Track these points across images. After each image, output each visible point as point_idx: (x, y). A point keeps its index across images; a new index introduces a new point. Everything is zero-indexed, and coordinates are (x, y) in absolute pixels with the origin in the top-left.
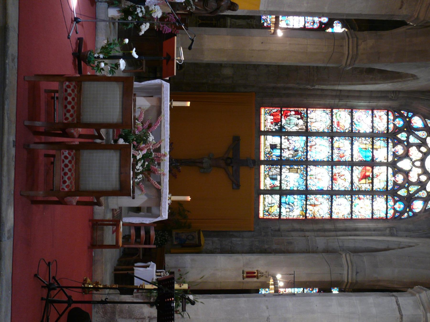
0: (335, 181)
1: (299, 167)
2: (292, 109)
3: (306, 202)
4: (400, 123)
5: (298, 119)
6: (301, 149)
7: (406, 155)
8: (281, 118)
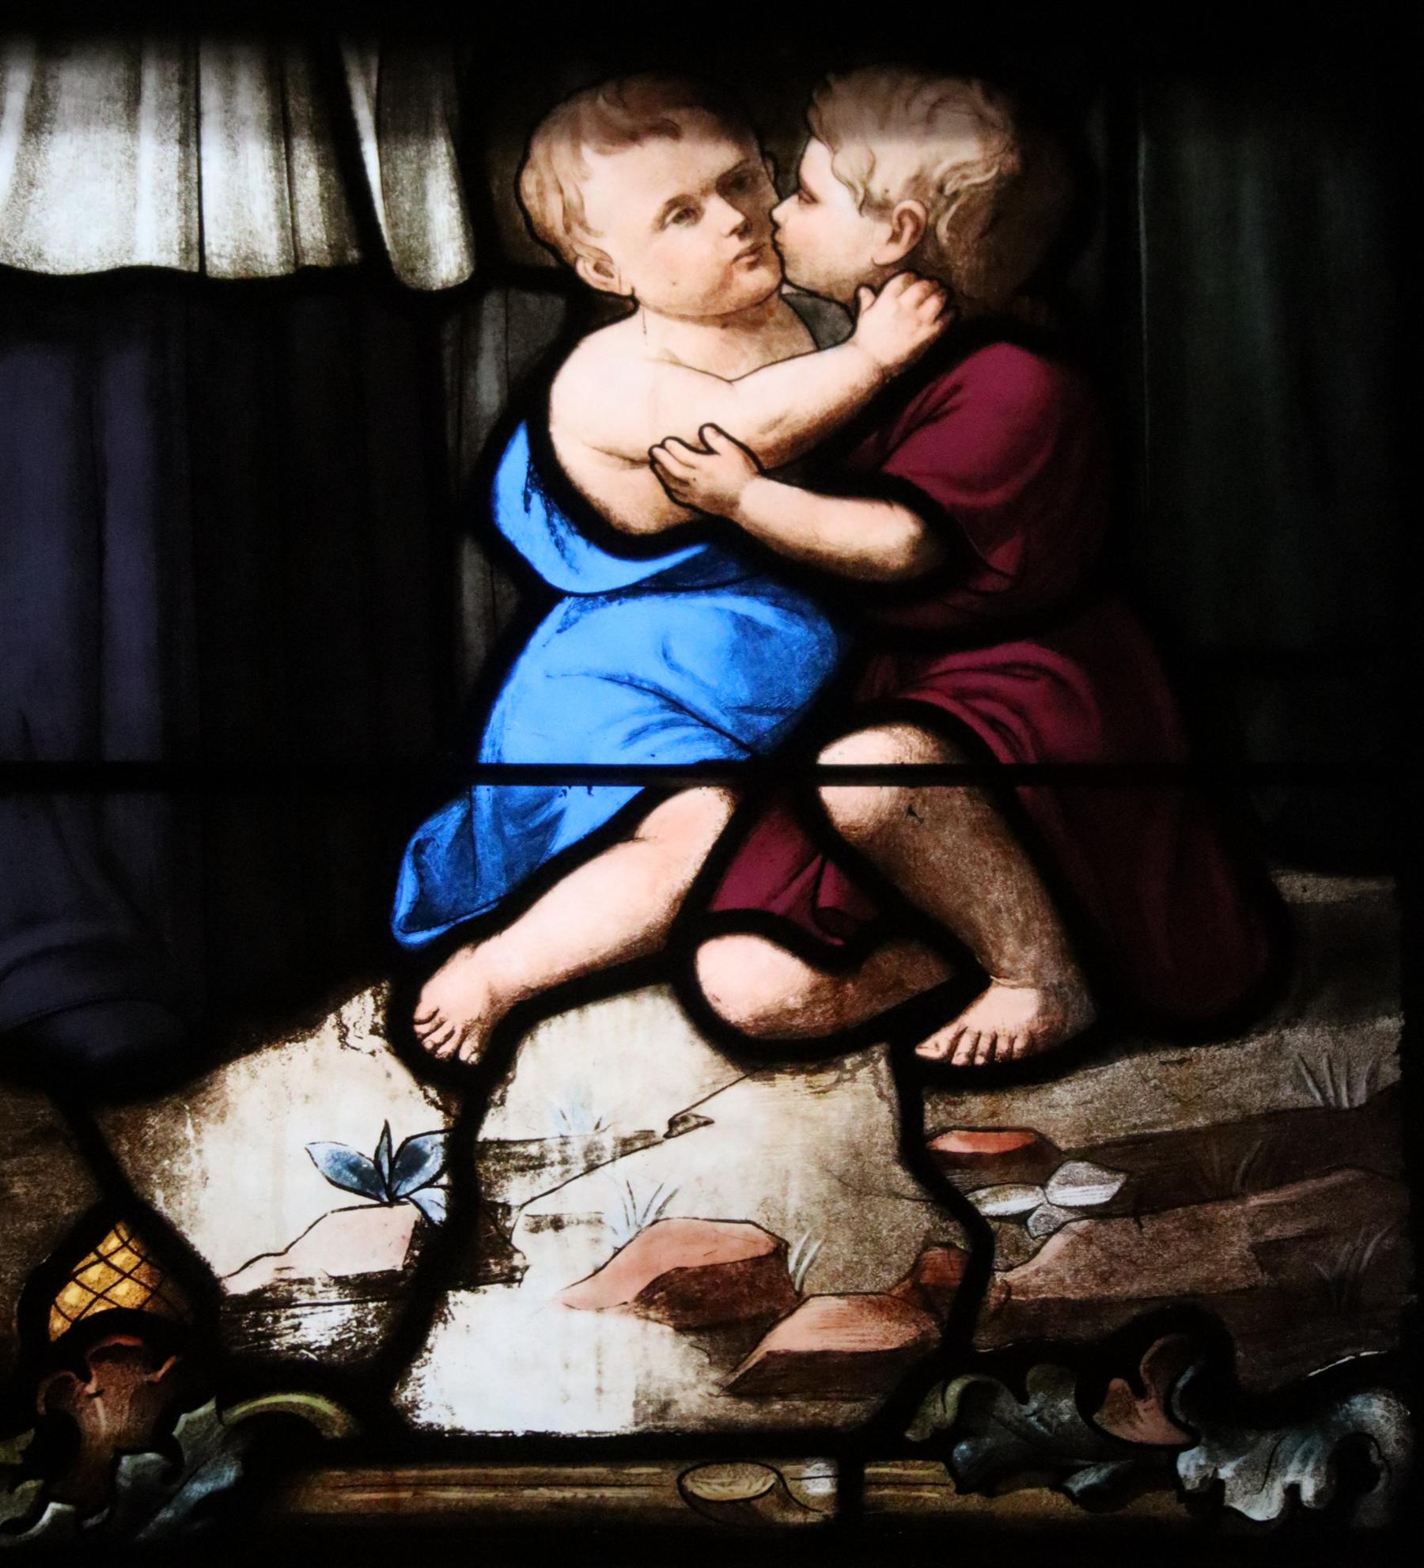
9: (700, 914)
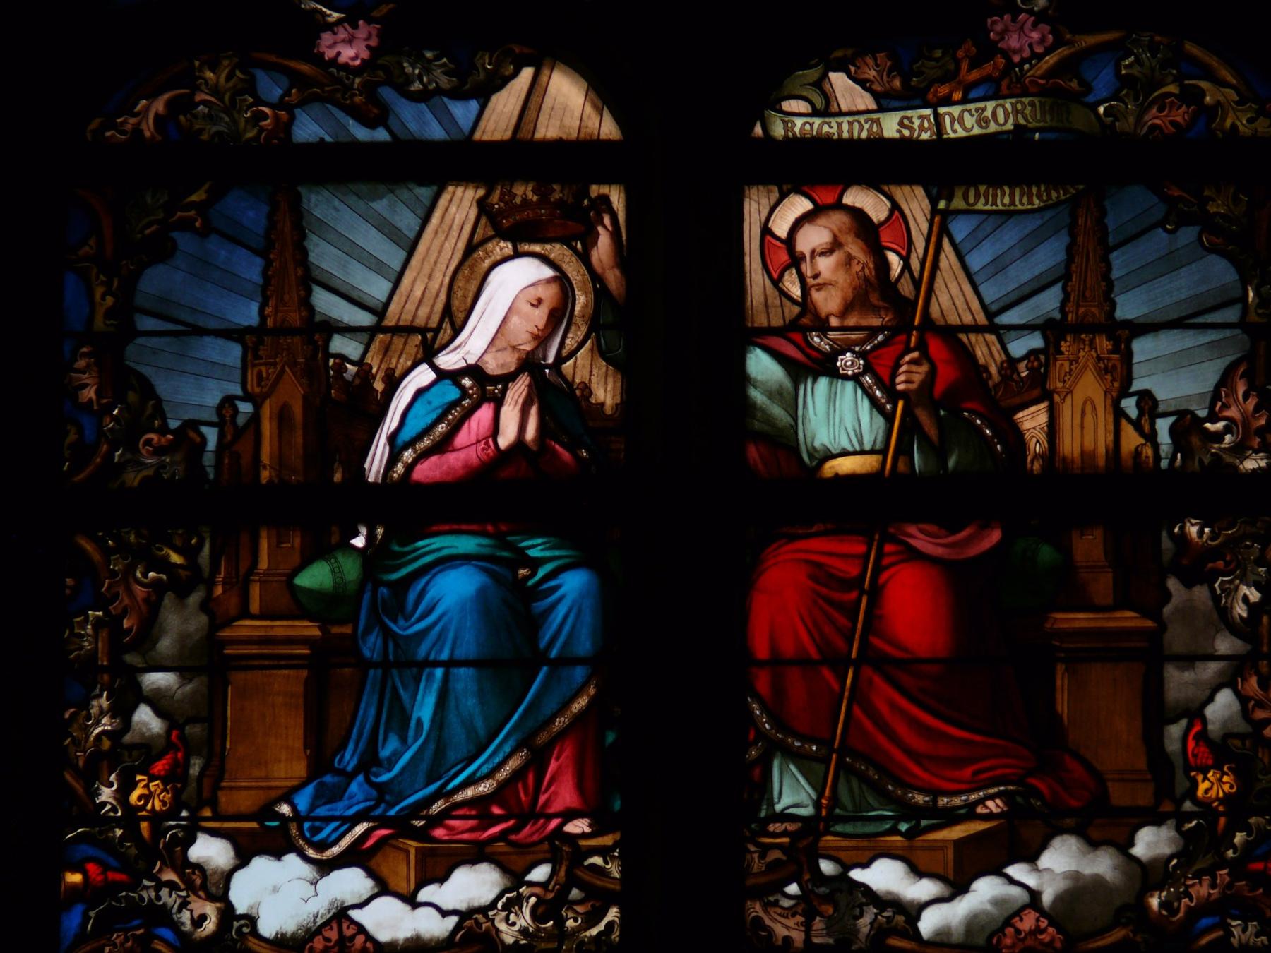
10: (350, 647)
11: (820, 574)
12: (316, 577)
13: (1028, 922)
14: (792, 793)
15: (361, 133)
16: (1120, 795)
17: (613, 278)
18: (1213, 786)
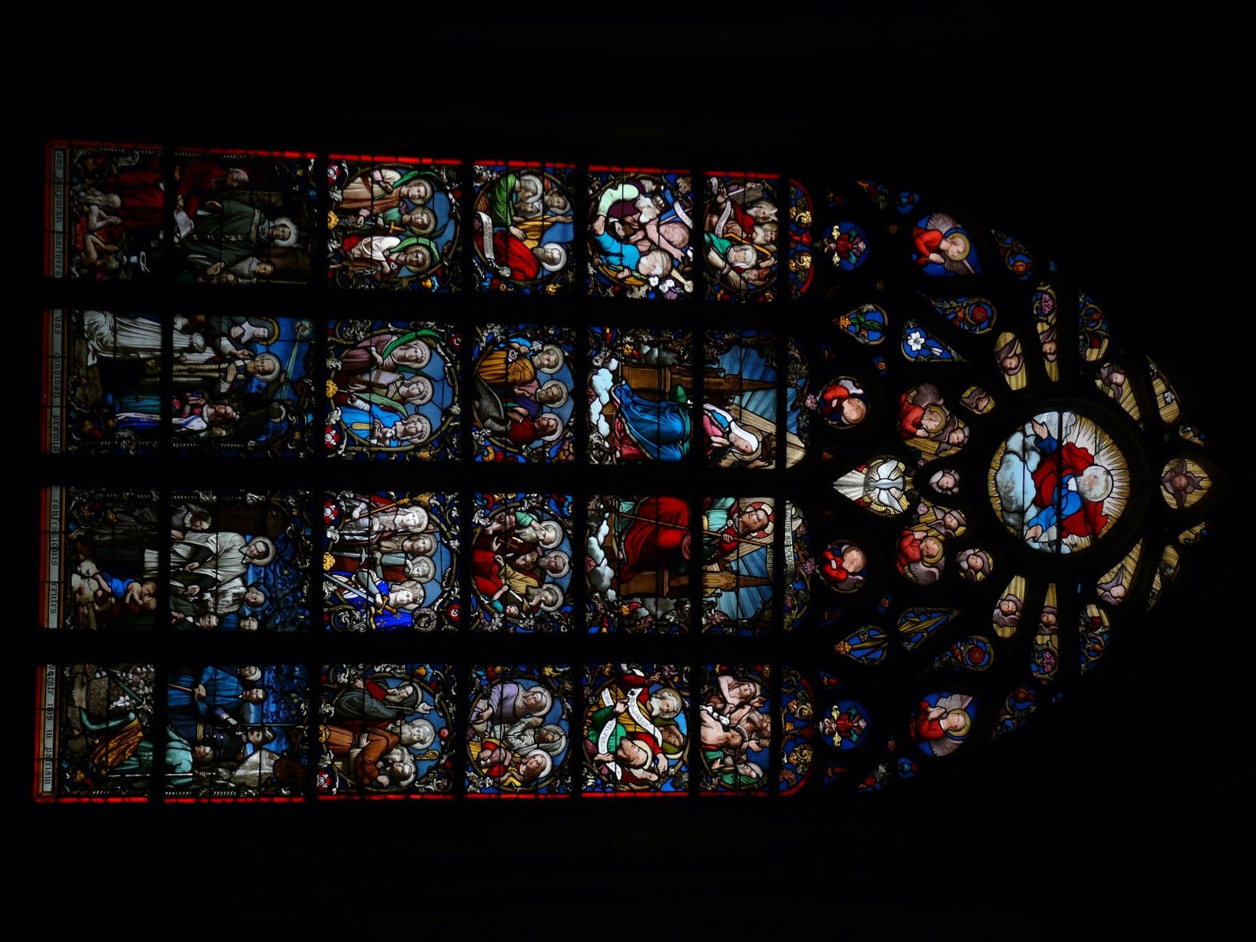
0: (484, 582)
1: (275, 500)
2: (230, 155)
3: (315, 707)
4: (845, 246)
5: (272, 213)
6: (285, 393)
7: (882, 437)
8: (171, 207)
9: (104, 590)
10: (664, 399)
11: (678, 516)
12: (681, 391)
13: (593, 564)
14: (625, 507)
15: (789, 405)
16: (623, 587)
17: (752, 466)
18: (625, 609)
